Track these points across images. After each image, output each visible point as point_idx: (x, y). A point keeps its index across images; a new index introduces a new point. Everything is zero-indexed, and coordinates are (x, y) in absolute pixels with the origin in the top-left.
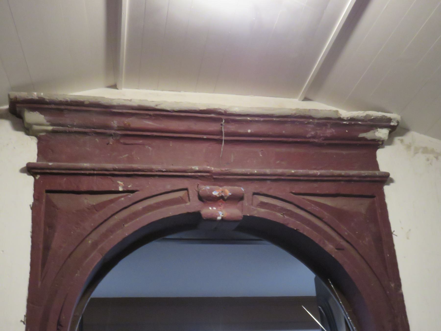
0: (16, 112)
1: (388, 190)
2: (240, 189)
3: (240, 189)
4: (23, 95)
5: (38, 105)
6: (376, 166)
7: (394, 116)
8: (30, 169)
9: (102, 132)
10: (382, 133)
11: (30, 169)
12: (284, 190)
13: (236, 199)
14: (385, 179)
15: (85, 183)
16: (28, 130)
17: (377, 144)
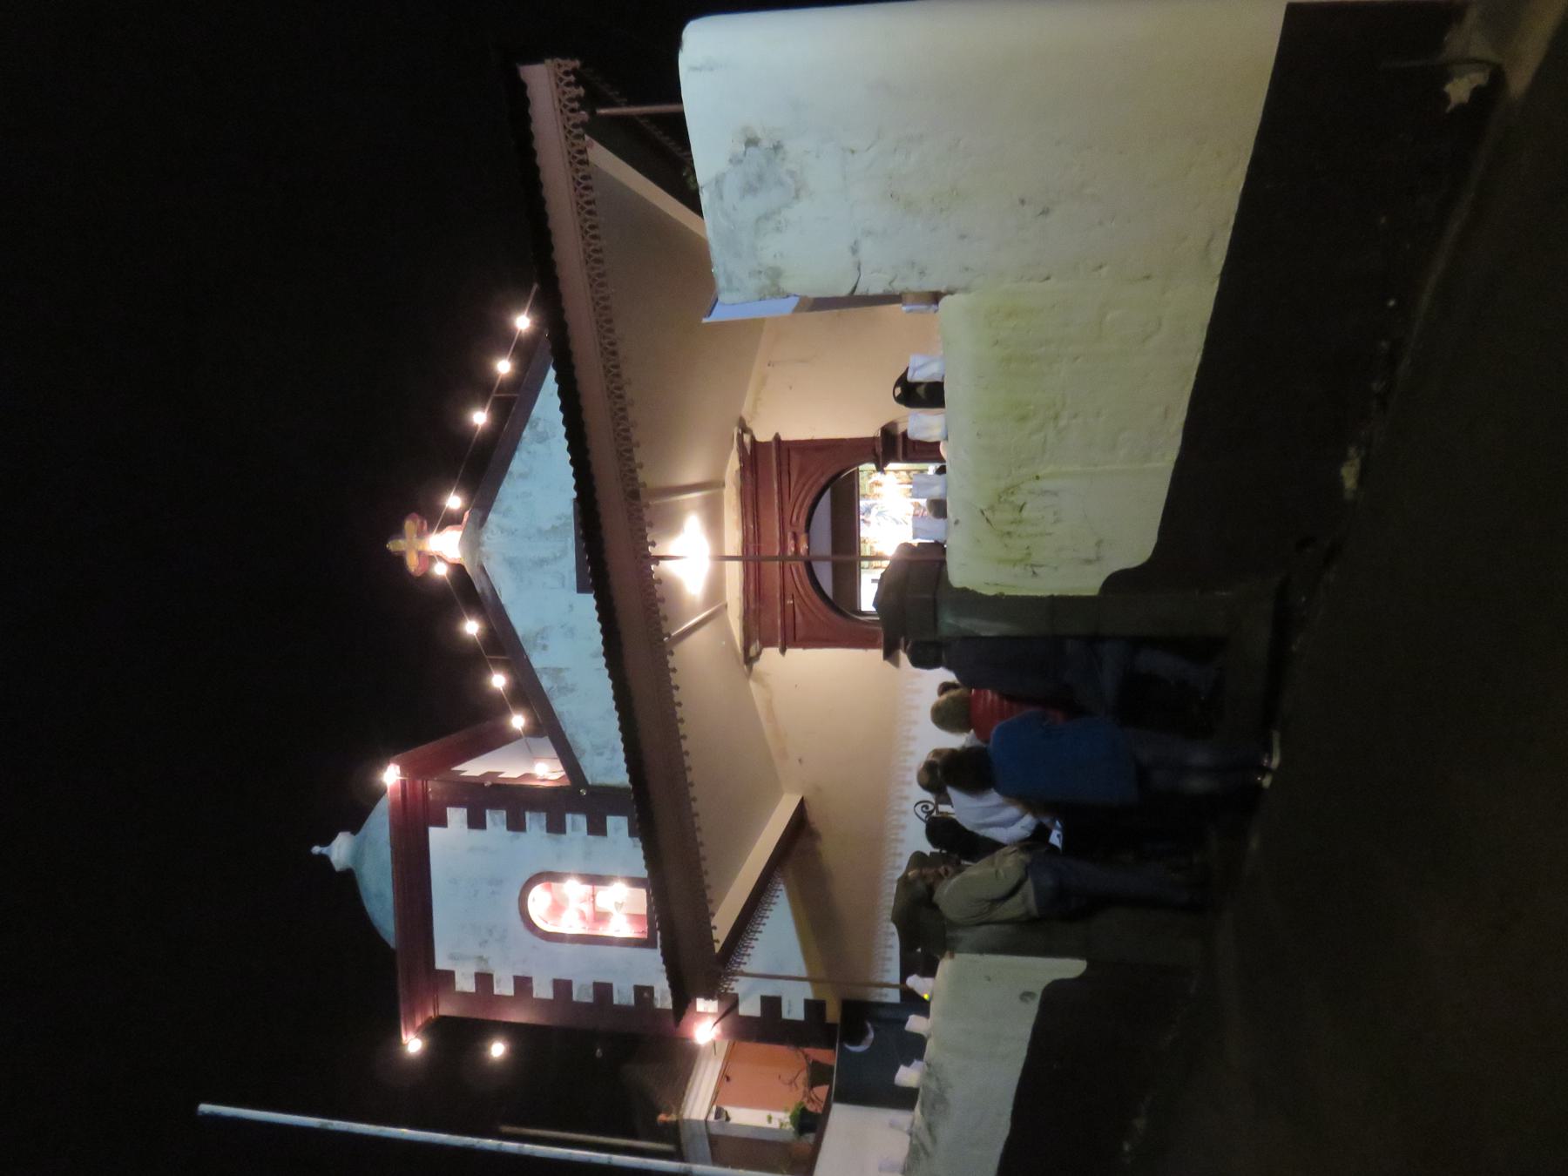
0: (749, 660)
1: (784, 438)
2: (789, 535)
3: (789, 535)
4: (742, 658)
5: (746, 649)
6: (766, 445)
7: (736, 431)
8: (783, 651)
9: (758, 613)
10: (747, 438)
11: (783, 651)
12: (788, 508)
13: (795, 537)
14: (777, 438)
15: (789, 621)
16: (759, 654)
17: (754, 442)
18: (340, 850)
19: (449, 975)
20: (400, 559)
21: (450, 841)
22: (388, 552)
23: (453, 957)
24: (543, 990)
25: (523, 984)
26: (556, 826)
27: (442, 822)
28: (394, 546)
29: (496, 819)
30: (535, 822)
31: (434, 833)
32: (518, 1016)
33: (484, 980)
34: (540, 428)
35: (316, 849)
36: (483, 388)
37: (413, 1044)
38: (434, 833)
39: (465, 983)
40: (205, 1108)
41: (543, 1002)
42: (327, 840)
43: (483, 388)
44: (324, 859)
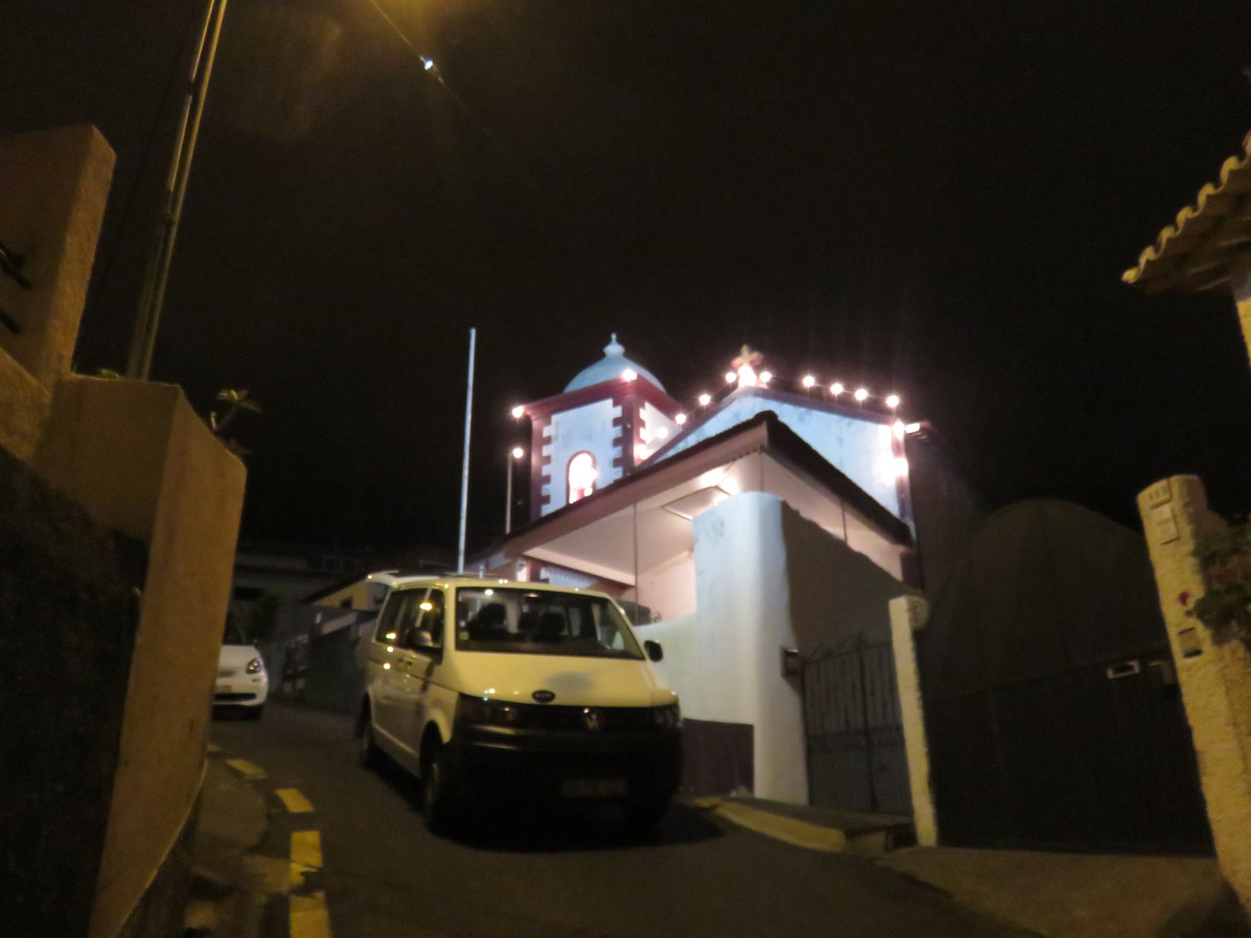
18: (614, 349)
19: (549, 422)
20: (737, 353)
21: (607, 410)
22: (740, 346)
23: (557, 423)
24: (546, 470)
25: (547, 460)
26: (616, 463)
27: (615, 404)
28: (745, 349)
29: (617, 432)
30: (617, 452)
31: (610, 402)
32: (534, 460)
33: (548, 441)
34: (807, 417)
35: (614, 336)
36: (825, 379)
37: (518, 412)
38: (610, 402)
39: (547, 432)
40: (473, 332)
41: (540, 471)
42: (620, 341)
43: (825, 379)
44: (608, 341)
